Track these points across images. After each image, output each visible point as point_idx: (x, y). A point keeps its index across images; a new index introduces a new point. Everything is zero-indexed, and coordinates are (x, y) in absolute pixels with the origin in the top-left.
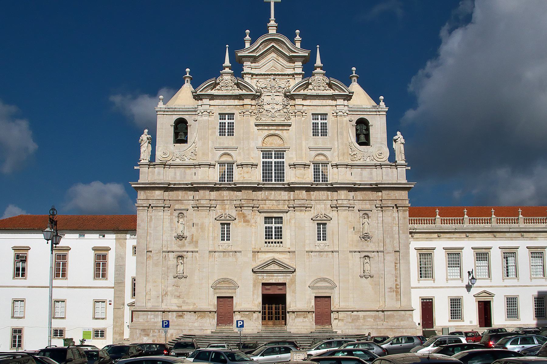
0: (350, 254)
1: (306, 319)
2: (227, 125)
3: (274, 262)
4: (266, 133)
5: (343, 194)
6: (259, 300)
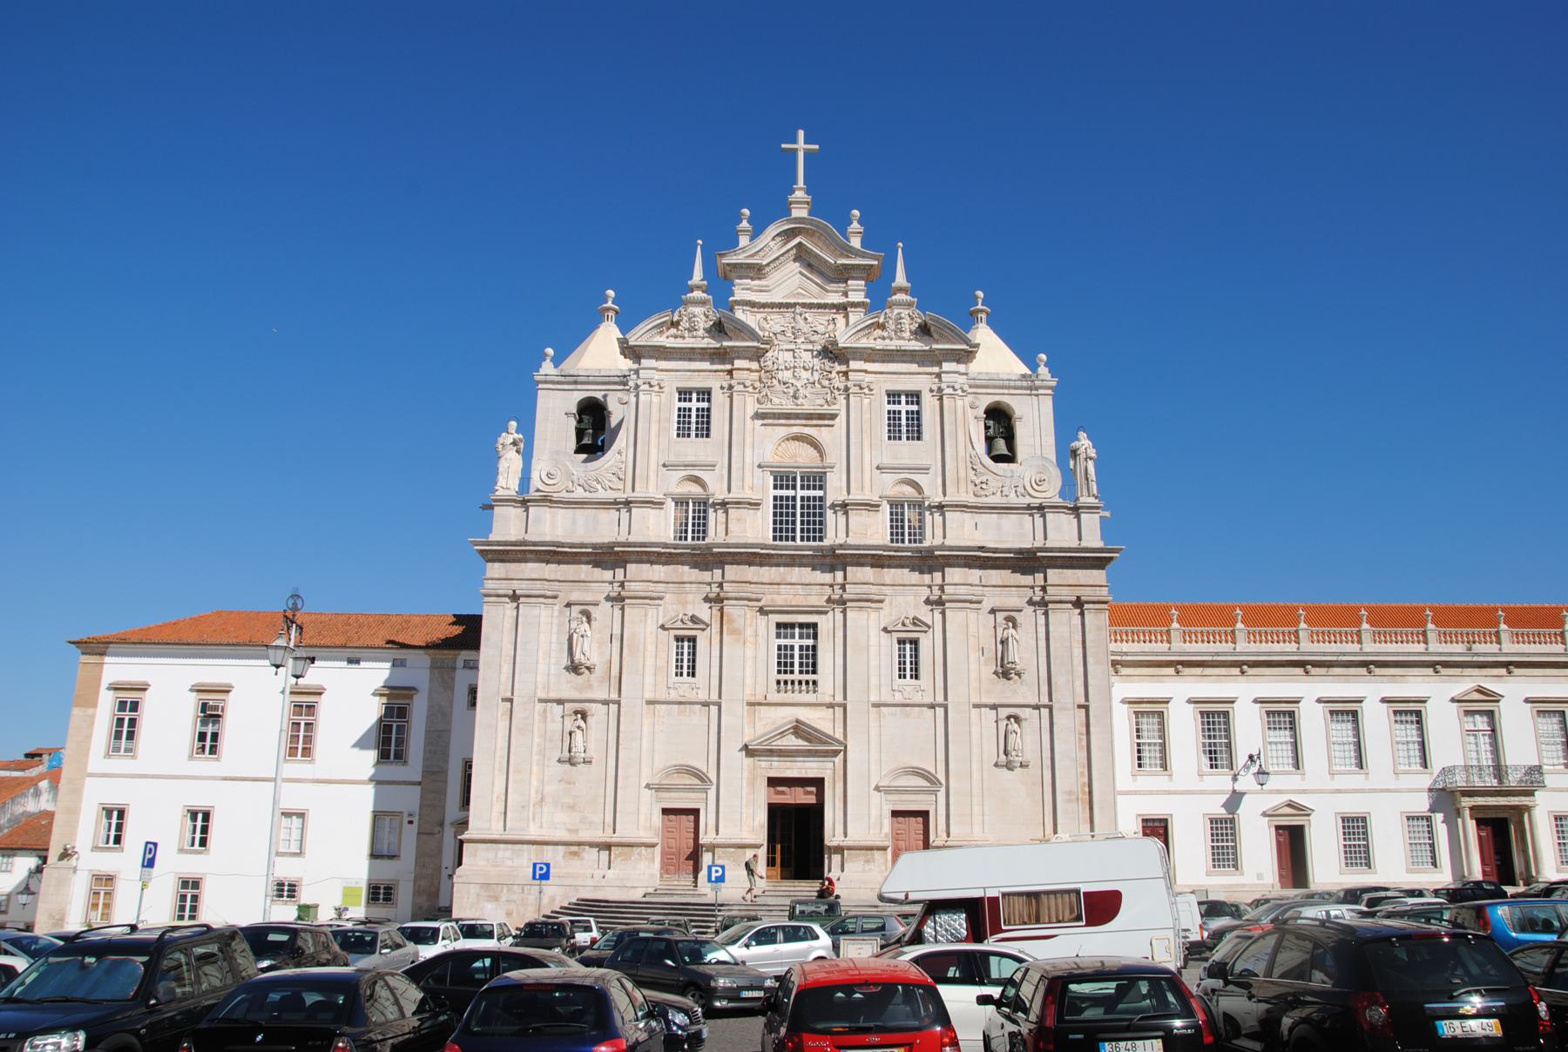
0: (975, 711)
1: (871, 866)
2: (694, 413)
3: (799, 729)
5: (955, 574)
6: (762, 817)
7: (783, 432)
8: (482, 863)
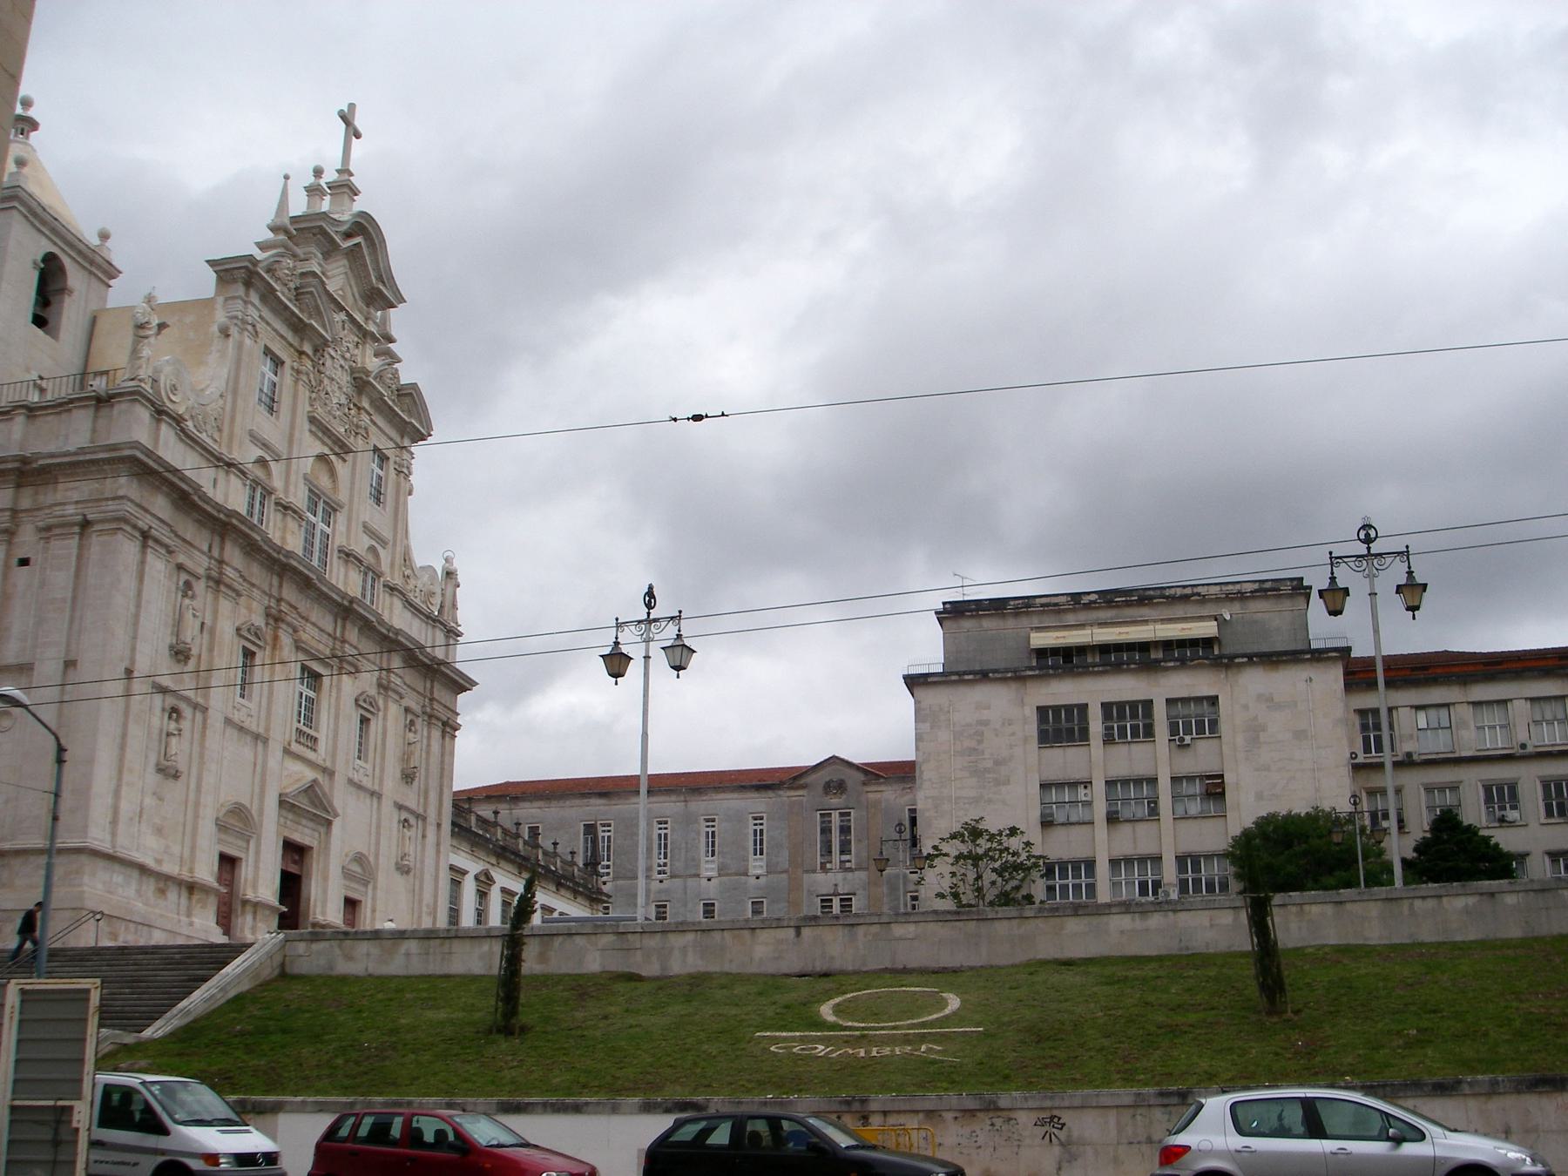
4: (319, 448)
7: (319, 448)
8: (100, 886)
